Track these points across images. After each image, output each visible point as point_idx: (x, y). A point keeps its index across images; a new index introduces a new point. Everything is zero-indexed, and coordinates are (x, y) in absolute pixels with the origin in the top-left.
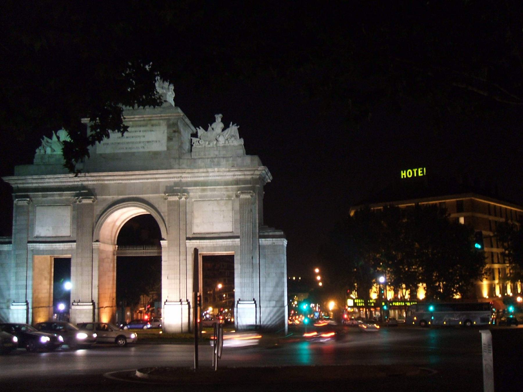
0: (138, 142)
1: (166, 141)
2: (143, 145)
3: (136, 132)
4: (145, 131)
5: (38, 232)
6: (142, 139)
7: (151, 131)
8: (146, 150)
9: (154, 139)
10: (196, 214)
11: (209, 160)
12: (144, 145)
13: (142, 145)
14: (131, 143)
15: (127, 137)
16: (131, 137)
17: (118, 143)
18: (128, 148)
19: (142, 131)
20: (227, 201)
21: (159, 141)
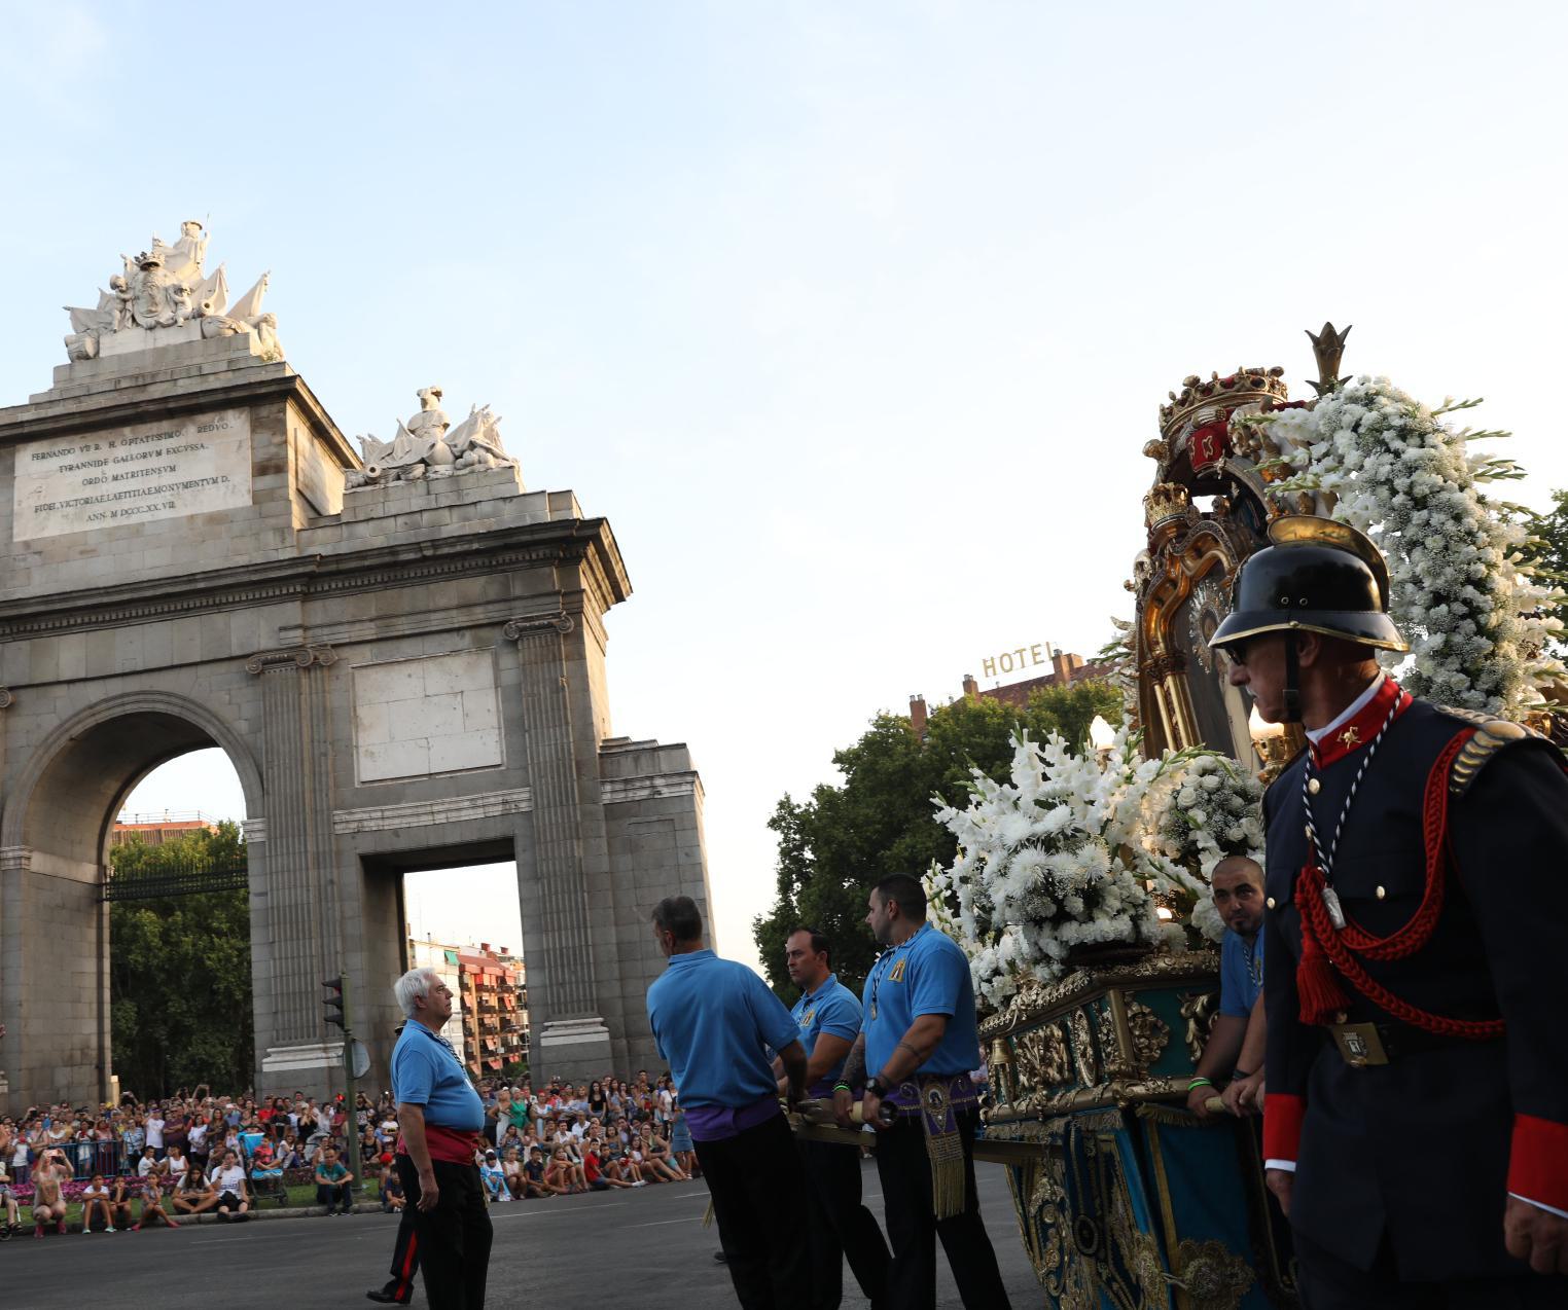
3: (144, 456)
4: (175, 451)
6: (168, 479)
7: (194, 447)
8: (182, 512)
9: (210, 473)
10: (362, 712)
11: (400, 520)
13: (167, 496)
15: (115, 478)
17: (87, 501)
18: (119, 513)
19: (164, 451)
20: (475, 657)
21: (225, 479)
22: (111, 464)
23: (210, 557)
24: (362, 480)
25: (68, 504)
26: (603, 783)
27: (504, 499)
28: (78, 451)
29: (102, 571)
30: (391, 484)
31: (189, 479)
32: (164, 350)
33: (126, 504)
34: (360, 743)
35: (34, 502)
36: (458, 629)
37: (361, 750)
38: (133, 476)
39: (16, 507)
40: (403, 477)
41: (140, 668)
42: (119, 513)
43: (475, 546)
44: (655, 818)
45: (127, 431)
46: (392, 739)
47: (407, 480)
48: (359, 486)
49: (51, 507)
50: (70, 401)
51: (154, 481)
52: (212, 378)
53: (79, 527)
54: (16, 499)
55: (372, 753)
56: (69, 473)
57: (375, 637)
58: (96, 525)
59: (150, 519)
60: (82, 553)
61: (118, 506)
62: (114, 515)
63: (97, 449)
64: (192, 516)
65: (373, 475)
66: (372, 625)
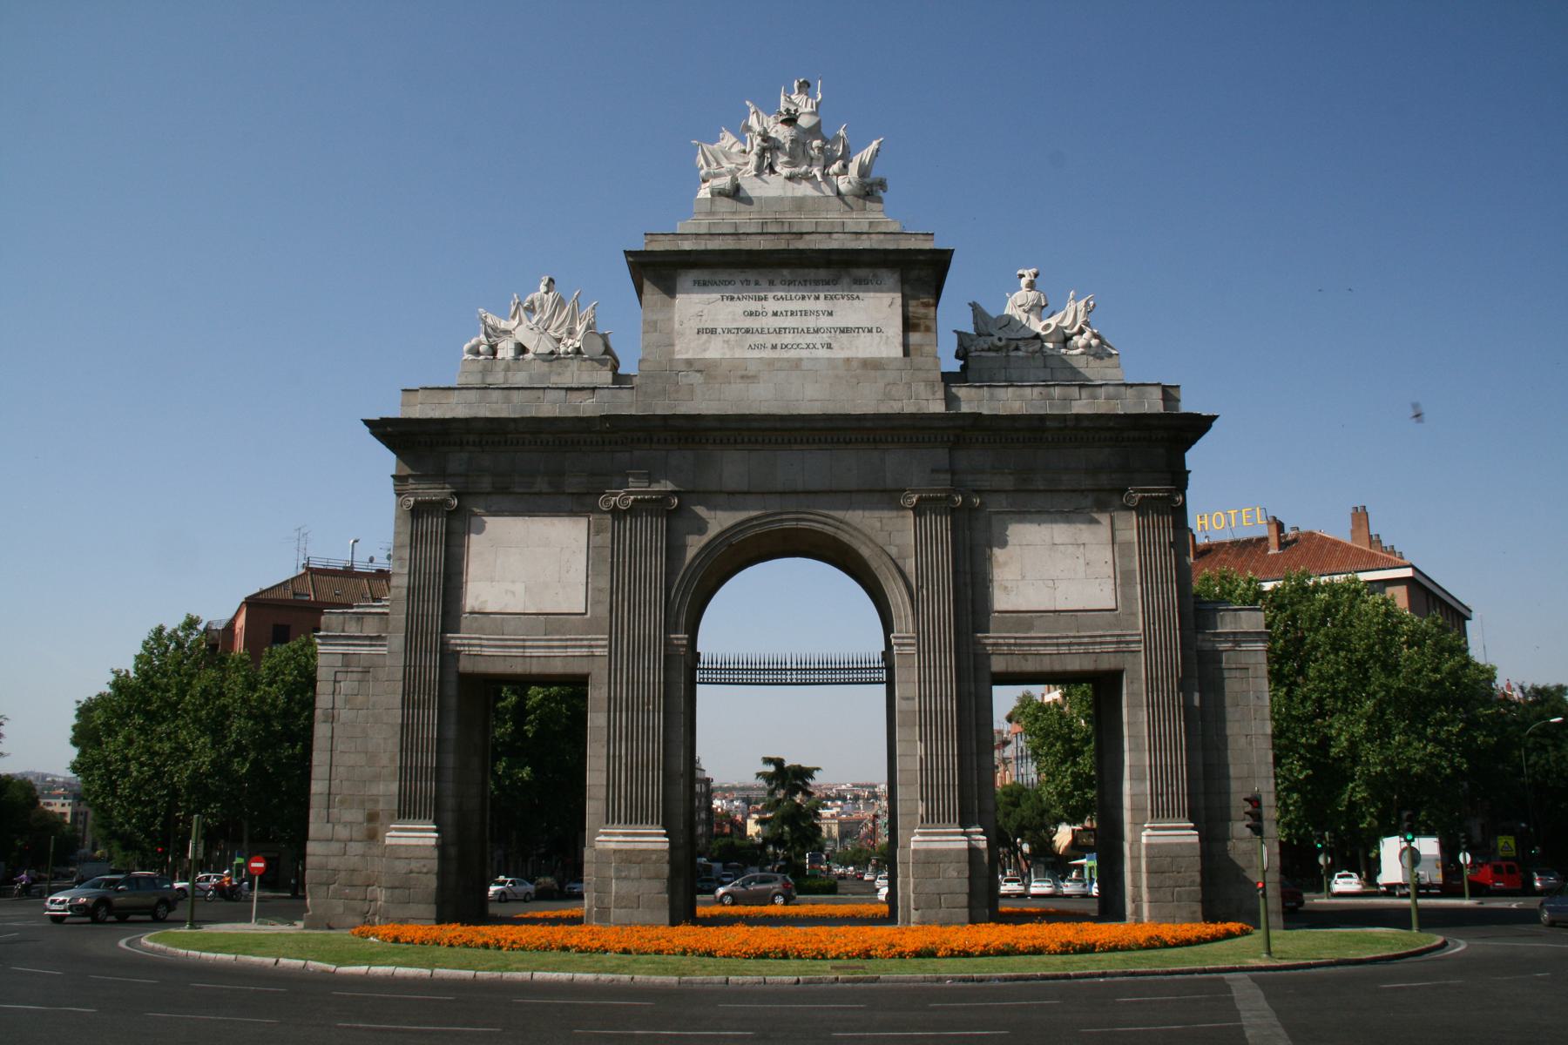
0: (812, 331)
1: (901, 329)
2: (829, 341)
5: (477, 598)
6: (825, 322)
8: (839, 353)
12: (829, 337)
13: (825, 337)
14: (787, 331)
15: (775, 314)
16: (789, 314)
17: (747, 331)
18: (779, 346)
21: (879, 330)
22: (771, 300)
23: (865, 401)
24: (986, 346)
25: (729, 331)
26: (1197, 633)
27: (1126, 385)
28: (738, 284)
29: (761, 399)
30: (1013, 354)
31: (843, 325)
32: (799, 204)
33: (788, 338)
34: (995, 578)
35: (695, 324)
36: (1083, 491)
37: (995, 584)
38: (792, 314)
39: (677, 326)
40: (1023, 348)
41: (800, 487)
42: (779, 346)
43: (1111, 424)
44: (1234, 666)
45: (786, 272)
46: (1023, 578)
47: (1027, 352)
48: (983, 350)
49: (713, 331)
50: (730, 237)
51: (811, 322)
52: (864, 237)
53: (738, 354)
54: (676, 318)
55: (1006, 588)
56: (729, 302)
57: (1011, 489)
58: (756, 354)
59: (809, 356)
60: (742, 377)
61: (774, 339)
62: (774, 347)
63: (757, 283)
64: (848, 359)
65: (1000, 344)
66: (1011, 477)
